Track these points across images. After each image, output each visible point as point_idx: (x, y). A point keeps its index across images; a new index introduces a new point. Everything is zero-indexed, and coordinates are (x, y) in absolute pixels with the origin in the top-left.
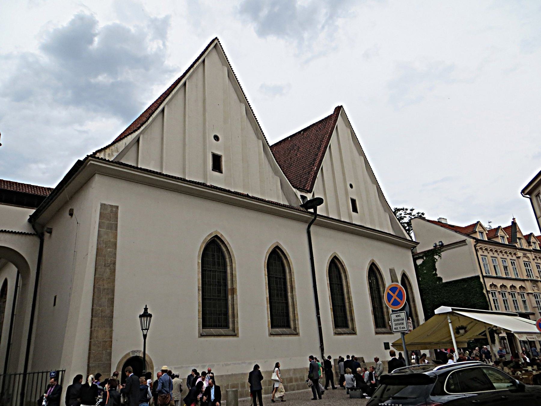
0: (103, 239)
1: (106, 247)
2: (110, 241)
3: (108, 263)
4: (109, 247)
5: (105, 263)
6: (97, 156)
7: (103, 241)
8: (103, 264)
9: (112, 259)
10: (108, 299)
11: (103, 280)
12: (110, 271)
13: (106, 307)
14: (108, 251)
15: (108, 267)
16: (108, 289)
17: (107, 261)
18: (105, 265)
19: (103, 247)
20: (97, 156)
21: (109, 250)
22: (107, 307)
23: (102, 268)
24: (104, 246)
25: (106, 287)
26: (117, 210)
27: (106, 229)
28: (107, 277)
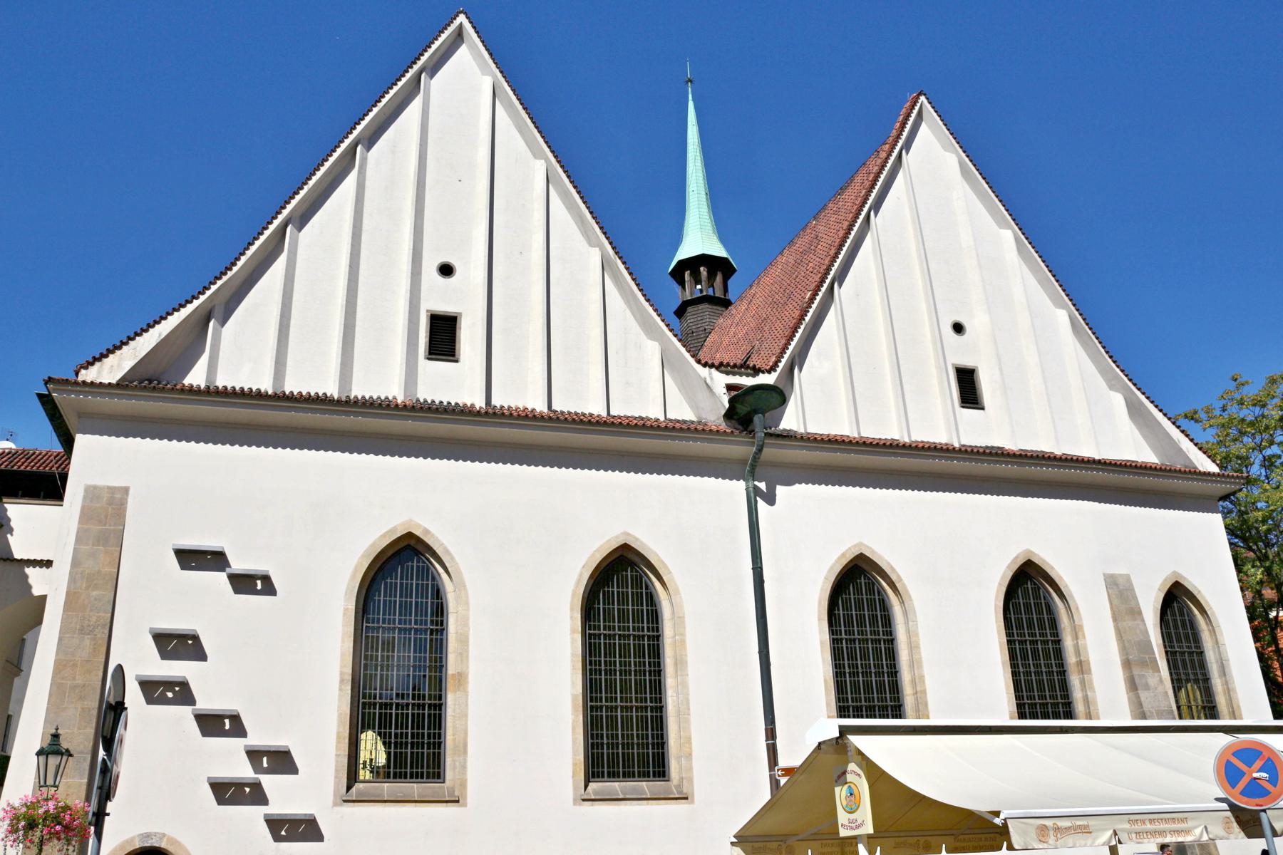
0: (82, 569)
1: (87, 588)
2: (99, 572)
3: (89, 626)
4: (96, 587)
5: (82, 626)
6: (80, 378)
7: (81, 574)
8: (78, 627)
9: (100, 614)
10: (83, 709)
11: (75, 665)
12: (93, 643)
13: (76, 729)
14: (92, 596)
15: (89, 634)
16: (84, 685)
17: (89, 620)
18: (82, 631)
19: (81, 589)
20: (80, 378)
21: (95, 593)
22: (79, 729)
23: (73, 637)
24: (84, 585)
25: (79, 681)
26: (125, 496)
27: (93, 545)
28: (83, 659)
